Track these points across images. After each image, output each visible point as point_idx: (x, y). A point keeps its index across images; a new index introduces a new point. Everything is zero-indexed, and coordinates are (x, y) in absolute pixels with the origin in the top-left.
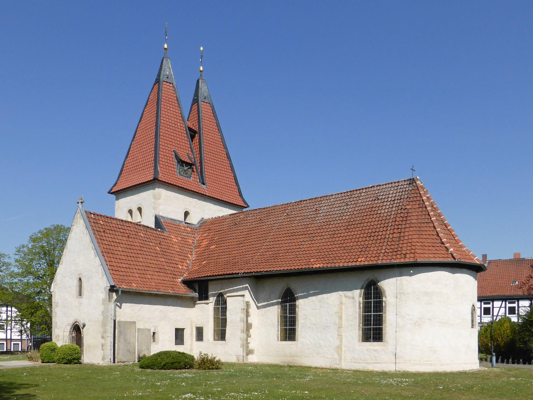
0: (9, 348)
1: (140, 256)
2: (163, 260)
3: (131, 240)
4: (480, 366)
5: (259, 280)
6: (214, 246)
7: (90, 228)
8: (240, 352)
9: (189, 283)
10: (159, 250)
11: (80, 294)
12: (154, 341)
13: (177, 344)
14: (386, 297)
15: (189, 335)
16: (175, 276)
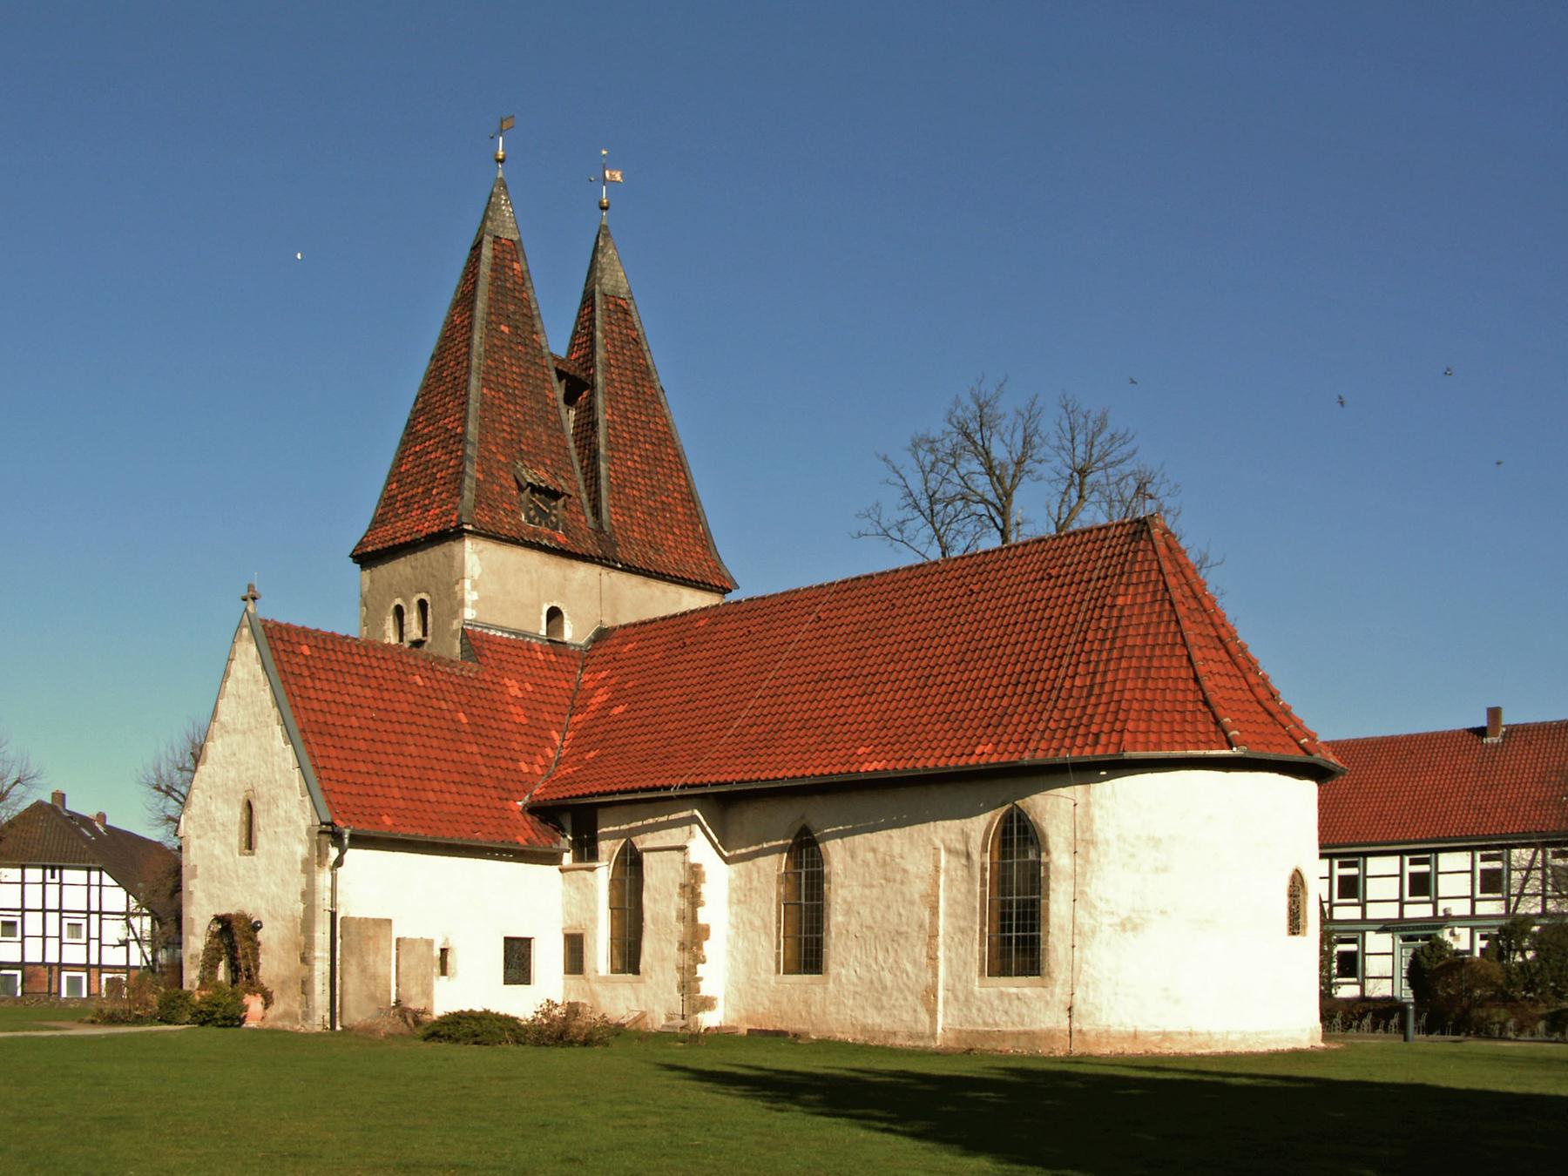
0: (94, 990)
1: (410, 740)
2: (475, 749)
3: (386, 696)
4: (1325, 1038)
5: (730, 808)
6: (621, 708)
7: (272, 667)
8: (675, 1000)
9: (546, 813)
10: (464, 720)
11: (249, 844)
12: (444, 972)
13: (509, 980)
14: (1048, 853)
15: (548, 959)
16: (511, 795)
